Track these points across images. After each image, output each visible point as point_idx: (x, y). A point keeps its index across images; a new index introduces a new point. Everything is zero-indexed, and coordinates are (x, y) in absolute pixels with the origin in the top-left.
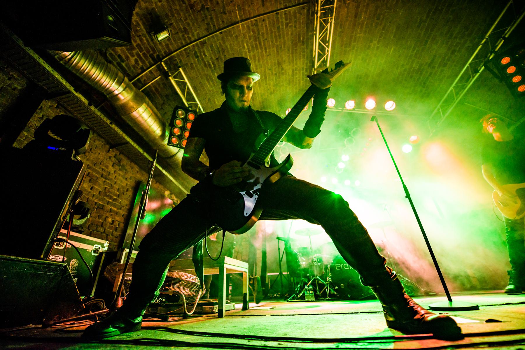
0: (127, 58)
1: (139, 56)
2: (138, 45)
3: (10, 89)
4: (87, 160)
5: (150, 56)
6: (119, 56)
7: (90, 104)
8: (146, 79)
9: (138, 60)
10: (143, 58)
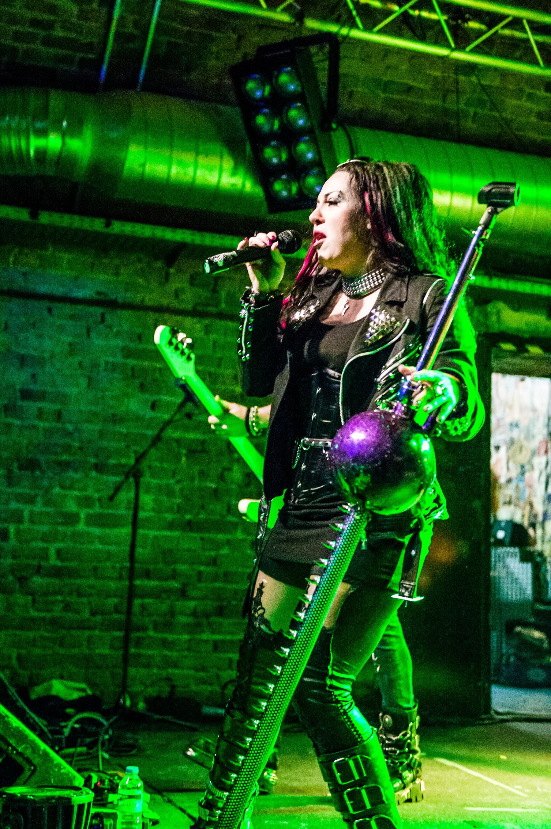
4: (117, 335)
6: (35, 23)
7: (34, 215)
8: (136, 17)
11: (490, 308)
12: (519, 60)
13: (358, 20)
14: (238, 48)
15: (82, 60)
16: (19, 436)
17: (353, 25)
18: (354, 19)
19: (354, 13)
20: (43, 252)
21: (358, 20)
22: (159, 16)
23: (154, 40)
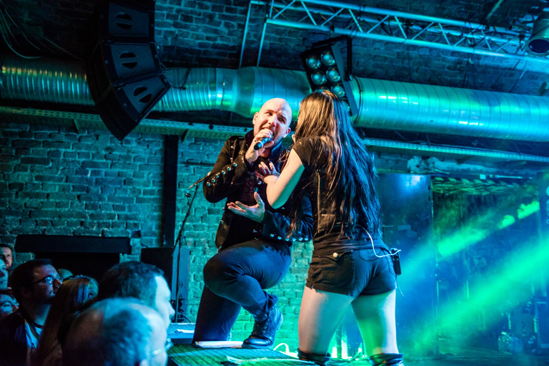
0: (216, 31)
1: (224, 17)
2: (214, 8)
3: (153, 156)
5: (235, 5)
6: (208, 38)
7: (211, 127)
8: (255, 33)
9: (228, 21)
10: (230, 14)
11: (429, 160)
12: (437, 42)
13: (360, 29)
14: (303, 44)
15: (230, 54)
16: (208, 231)
17: (358, 30)
18: (358, 28)
19: (358, 25)
20: (216, 145)
21: (360, 29)
22: (266, 31)
23: (264, 43)
